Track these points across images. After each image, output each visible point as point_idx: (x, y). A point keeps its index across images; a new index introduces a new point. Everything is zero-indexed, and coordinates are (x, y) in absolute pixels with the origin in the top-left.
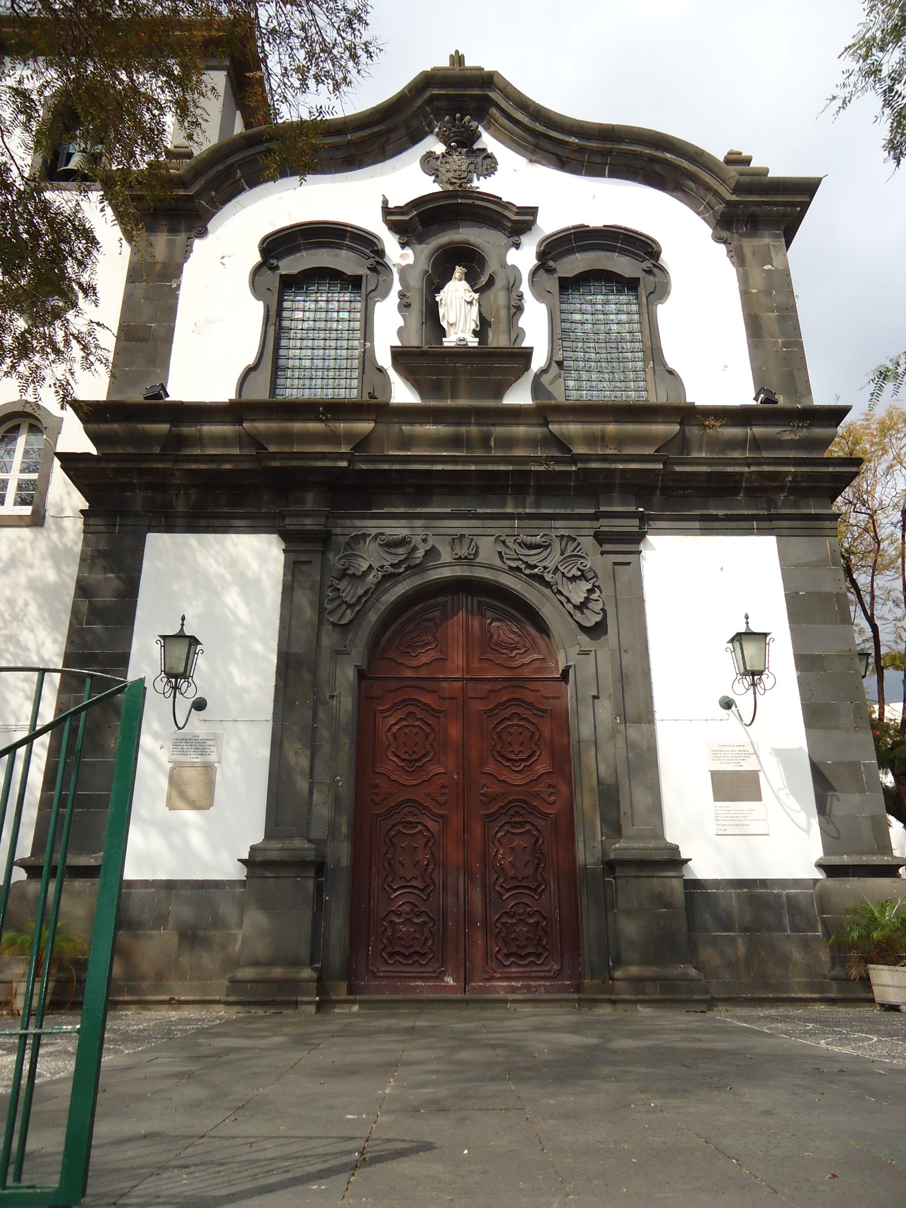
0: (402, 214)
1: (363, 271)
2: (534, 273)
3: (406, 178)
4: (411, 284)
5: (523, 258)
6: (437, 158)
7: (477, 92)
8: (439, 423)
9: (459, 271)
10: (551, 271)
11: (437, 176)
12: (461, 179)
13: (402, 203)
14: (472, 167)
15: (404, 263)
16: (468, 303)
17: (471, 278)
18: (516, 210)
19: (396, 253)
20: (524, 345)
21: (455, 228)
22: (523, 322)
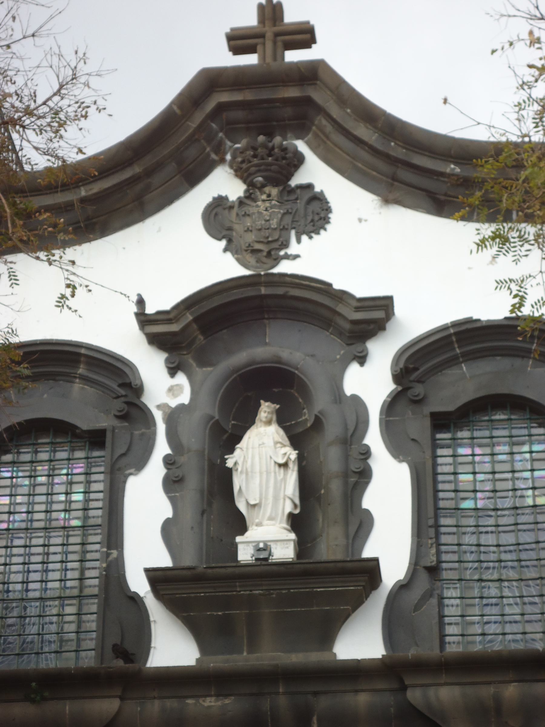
0: (169, 321)
1: (104, 422)
2: (391, 407)
3: (176, 254)
4: (185, 440)
5: (370, 382)
6: (231, 207)
7: (292, 92)
8: (226, 696)
9: (266, 409)
10: (418, 402)
11: (230, 241)
12: (269, 242)
13: (167, 306)
14: (288, 219)
15: (174, 403)
16: (280, 465)
17: (283, 420)
18: (355, 304)
19: (163, 387)
20: (367, 553)
21: (257, 340)
22: (369, 501)
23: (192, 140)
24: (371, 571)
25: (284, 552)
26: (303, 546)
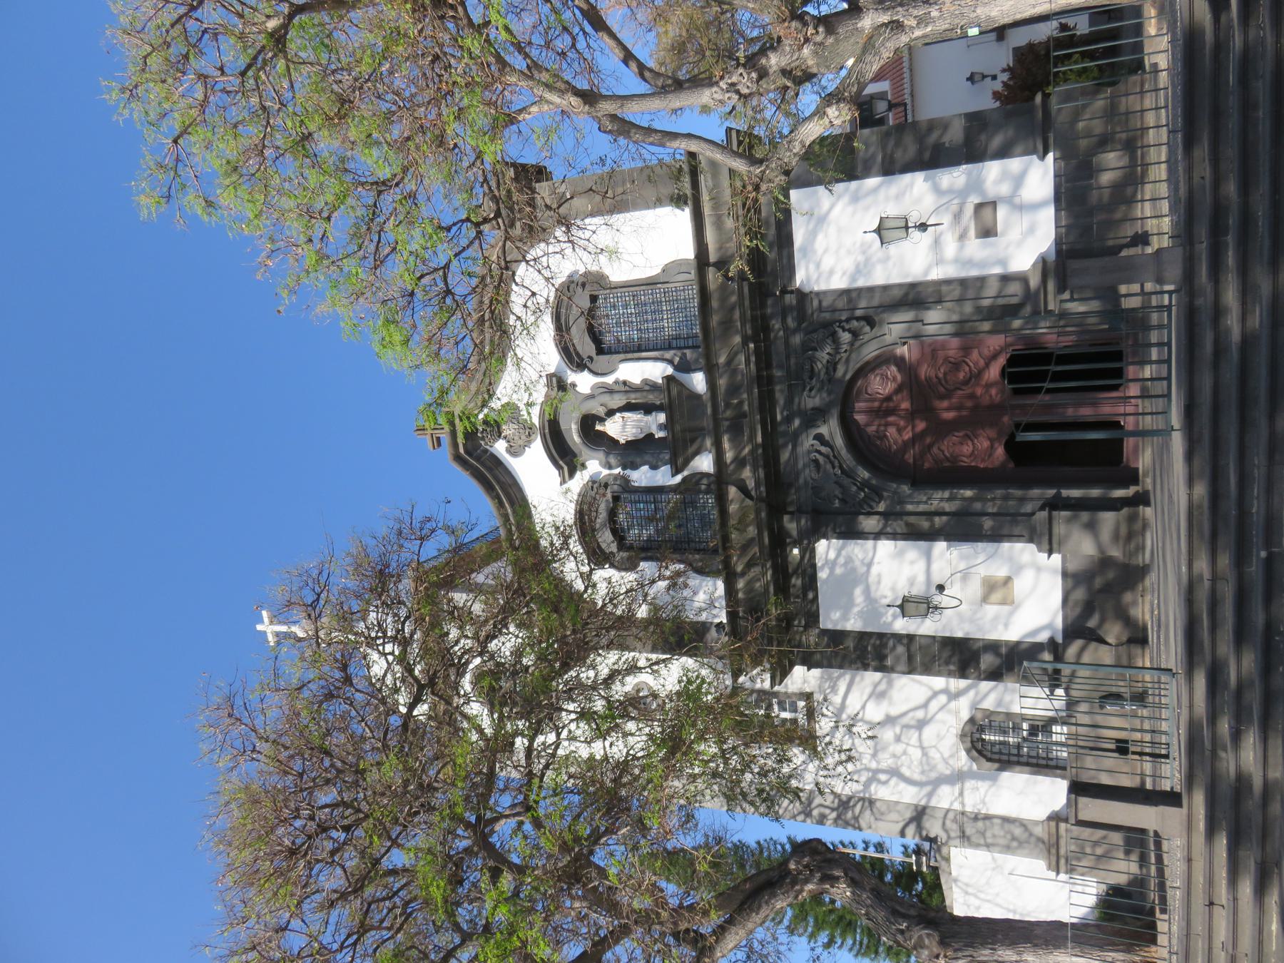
2: (596, 374)
3: (533, 470)
5: (584, 382)
9: (598, 427)
17: (602, 420)
20: (660, 381)
22: (636, 380)
23: (483, 464)
24: (669, 379)
25: (662, 417)
26: (659, 408)
